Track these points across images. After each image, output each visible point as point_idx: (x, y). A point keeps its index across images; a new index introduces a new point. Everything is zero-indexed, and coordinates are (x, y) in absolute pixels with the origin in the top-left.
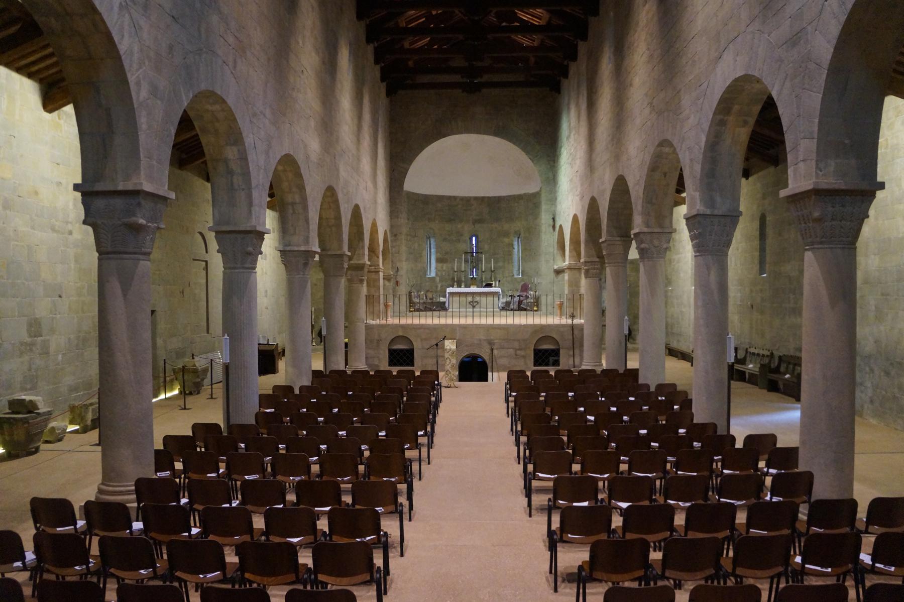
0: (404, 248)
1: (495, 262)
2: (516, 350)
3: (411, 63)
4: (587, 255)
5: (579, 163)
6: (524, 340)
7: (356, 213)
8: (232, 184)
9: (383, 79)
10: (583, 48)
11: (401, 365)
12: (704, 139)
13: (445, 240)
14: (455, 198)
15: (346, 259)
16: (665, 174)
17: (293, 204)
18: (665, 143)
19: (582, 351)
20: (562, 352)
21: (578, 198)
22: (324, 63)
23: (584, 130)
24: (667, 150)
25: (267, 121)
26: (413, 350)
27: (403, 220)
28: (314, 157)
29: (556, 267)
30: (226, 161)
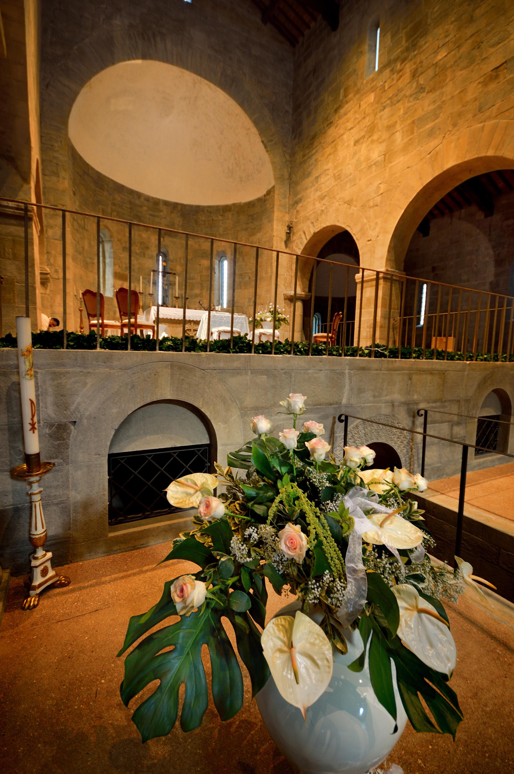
6: (467, 401)
14: (139, 195)
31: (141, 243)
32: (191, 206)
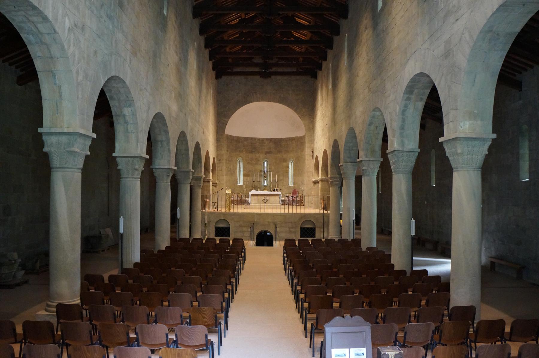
0: (224, 168)
1: (278, 176)
2: (290, 228)
3: (230, 60)
4: (332, 173)
5: (327, 120)
7: (197, 147)
8: (127, 130)
9: (213, 70)
10: (330, 54)
11: (222, 236)
12: (398, 108)
13: (248, 163)
14: (255, 139)
15: (191, 173)
16: (377, 127)
17: (162, 141)
18: (377, 109)
19: (328, 229)
20: (317, 230)
21: (327, 140)
22: (180, 60)
23: (330, 101)
24: (378, 113)
25: (148, 94)
26: (229, 228)
27: (224, 151)
28: (174, 115)
29: (314, 180)
30: (124, 116)
31: (256, 159)
32: (278, 139)
